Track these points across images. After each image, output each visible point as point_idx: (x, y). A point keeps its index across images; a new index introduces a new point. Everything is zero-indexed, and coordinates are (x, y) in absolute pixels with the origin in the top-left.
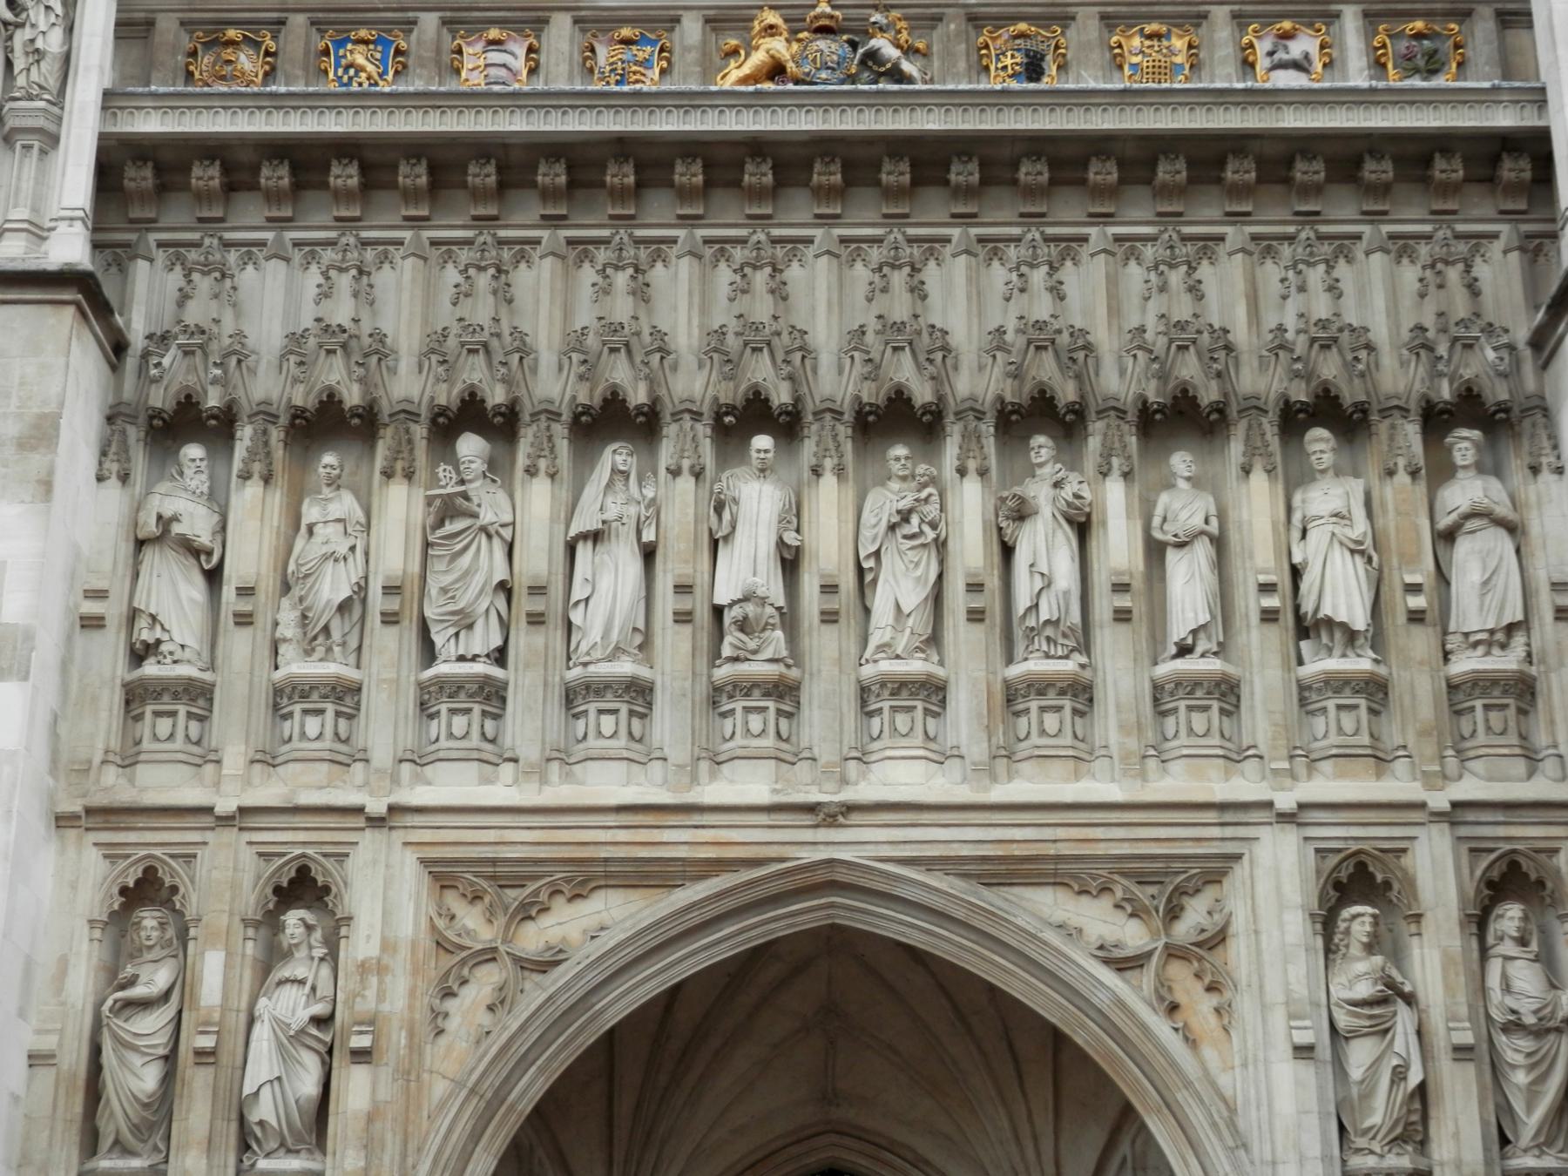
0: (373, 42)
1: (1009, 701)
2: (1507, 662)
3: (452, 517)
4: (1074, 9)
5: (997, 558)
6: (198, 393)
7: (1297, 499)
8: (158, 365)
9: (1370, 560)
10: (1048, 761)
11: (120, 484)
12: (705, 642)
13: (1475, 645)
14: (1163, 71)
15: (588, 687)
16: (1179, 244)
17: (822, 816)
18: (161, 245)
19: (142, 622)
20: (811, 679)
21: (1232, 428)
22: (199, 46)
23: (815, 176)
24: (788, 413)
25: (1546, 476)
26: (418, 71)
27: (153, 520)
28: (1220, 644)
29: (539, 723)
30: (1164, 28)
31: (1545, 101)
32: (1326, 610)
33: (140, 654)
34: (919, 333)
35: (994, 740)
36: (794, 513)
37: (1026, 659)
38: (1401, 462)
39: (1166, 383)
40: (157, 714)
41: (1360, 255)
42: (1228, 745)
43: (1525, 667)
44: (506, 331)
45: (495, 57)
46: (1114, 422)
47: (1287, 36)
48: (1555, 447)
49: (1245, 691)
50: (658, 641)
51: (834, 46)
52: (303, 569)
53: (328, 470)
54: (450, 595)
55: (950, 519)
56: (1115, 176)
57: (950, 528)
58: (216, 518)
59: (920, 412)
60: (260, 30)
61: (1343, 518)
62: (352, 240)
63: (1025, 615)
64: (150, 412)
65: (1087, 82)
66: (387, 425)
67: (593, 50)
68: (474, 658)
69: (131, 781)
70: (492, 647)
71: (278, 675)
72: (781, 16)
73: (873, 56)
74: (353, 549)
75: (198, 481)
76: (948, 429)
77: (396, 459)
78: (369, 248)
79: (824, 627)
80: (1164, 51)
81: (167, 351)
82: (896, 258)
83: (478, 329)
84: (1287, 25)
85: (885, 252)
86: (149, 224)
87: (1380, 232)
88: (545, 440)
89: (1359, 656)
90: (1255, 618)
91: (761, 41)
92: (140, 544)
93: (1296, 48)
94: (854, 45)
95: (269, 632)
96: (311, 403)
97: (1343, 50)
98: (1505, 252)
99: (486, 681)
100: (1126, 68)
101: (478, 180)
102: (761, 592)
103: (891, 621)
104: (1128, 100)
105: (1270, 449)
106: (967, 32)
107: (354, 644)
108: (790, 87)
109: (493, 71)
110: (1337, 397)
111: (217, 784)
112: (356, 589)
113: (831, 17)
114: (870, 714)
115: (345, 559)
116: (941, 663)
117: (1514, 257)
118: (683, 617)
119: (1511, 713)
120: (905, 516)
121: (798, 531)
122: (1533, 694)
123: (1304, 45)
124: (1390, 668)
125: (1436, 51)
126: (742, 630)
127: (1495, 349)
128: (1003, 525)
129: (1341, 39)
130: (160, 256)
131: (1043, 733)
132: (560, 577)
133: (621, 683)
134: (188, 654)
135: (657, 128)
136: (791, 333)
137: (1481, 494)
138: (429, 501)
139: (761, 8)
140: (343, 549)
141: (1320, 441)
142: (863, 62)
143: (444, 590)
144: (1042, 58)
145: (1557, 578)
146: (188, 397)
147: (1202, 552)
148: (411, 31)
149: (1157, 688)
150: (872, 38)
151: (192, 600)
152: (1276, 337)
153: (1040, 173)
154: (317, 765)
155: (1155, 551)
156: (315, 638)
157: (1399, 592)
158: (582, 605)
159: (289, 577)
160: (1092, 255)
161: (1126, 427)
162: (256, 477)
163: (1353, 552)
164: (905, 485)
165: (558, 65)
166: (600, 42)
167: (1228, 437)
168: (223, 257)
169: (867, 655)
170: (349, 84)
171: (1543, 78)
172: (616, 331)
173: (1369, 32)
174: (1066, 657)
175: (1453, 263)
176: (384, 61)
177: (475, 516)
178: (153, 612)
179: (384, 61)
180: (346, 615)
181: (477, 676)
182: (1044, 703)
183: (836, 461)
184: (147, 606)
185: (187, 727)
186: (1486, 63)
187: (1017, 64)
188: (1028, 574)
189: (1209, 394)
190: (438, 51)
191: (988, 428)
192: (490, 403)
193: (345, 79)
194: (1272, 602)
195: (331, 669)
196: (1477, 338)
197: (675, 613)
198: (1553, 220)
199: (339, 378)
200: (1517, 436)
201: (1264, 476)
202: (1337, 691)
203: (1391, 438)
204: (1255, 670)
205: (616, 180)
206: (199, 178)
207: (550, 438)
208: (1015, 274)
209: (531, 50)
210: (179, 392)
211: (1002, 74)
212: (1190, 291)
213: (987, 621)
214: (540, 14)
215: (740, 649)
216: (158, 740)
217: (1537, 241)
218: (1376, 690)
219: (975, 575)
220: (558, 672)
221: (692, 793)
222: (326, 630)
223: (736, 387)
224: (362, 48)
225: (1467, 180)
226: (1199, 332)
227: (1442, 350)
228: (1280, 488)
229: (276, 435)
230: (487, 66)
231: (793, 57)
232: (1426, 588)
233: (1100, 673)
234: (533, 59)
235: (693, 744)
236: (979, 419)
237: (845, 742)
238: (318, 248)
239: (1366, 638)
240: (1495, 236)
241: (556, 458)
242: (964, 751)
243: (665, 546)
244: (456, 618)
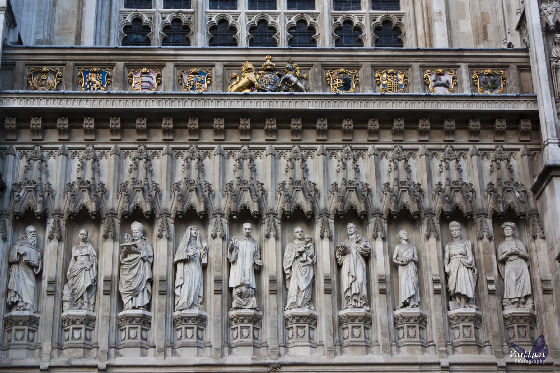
0: (99, 73)
1: (340, 324)
2: (526, 309)
3: (130, 254)
4: (362, 63)
5: (335, 270)
6: (33, 206)
7: (447, 248)
8: (18, 196)
9: (474, 271)
10: (355, 347)
11: (3, 241)
12: (226, 301)
13: (514, 303)
14: (395, 87)
15: (182, 319)
16: (401, 152)
17: (271, 368)
18: (18, 149)
19: (11, 294)
20: (266, 316)
21: (422, 221)
22: (32, 73)
23: (266, 125)
24: (257, 215)
25: (539, 240)
26: (116, 84)
27: (16, 255)
28: (419, 302)
29: (164, 333)
30: (395, 71)
31: (537, 101)
32: (458, 290)
33: (10, 306)
34: (306, 185)
35: (335, 339)
36: (259, 252)
37: (347, 308)
38: (485, 234)
39: (397, 205)
40: (17, 330)
41: (469, 157)
42: (423, 341)
43: (532, 312)
44: (150, 183)
45: (145, 79)
46: (379, 218)
47: (441, 74)
48: (542, 229)
49: (428, 320)
50: (208, 301)
51: (273, 76)
52: (73, 274)
53: (83, 236)
54: (129, 283)
55: (317, 255)
56: (378, 126)
57: (318, 258)
58: (39, 254)
59: (306, 214)
60: (56, 68)
61: (464, 255)
62: (91, 148)
63: (346, 291)
64: (15, 214)
65: (367, 91)
66: (105, 218)
67: (182, 76)
68: (139, 308)
69: (7, 356)
70: (145, 304)
71: (63, 315)
72: (252, 64)
73: (287, 80)
74: (92, 266)
75: (31, 240)
76: (316, 221)
77: (109, 231)
78: (97, 151)
79: (271, 296)
80: (395, 79)
81: (21, 190)
82: (296, 156)
83: (140, 182)
84: (440, 70)
85: (292, 154)
86: (15, 141)
87: (476, 148)
88: (165, 225)
89: (471, 307)
90: (432, 293)
91: (245, 74)
92: (10, 264)
93: (444, 79)
94: (280, 76)
95: (60, 298)
96: (77, 210)
97: (461, 79)
98: (522, 156)
99: (144, 316)
100: (381, 85)
101: (139, 126)
102: (247, 283)
103: (296, 294)
104: (383, 99)
105: (436, 229)
106: (322, 72)
107: (92, 302)
108: (256, 92)
109: (144, 84)
110: (461, 210)
111: (40, 357)
112: (93, 281)
113: (271, 65)
114: (289, 329)
115: (89, 270)
116: (315, 309)
117: (525, 158)
118: (217, 292)
119: (527, 329)
120: (301, 254)
121: (260, 259)
122: (536, 322)
123: (447, 77)
124: (482, 312)
125: (495, 81)
126: (240, 297)
127: (519, 192)
128: (338, 257)
129: (460, 76)
130: (18, 153)
131: (353, 336)
132: (171, 277)
133: (195, 317)
134: (28, 307)
135: (207, 107)
136: (257, 184)
137: (515, 247)
138: (122, 247)
139: (245, 61)
140: (88, 266)
141: (455, 226)
142: (283, 82)
143: (127, 282)
144: (350, 81)
145: (543, 278)
146: (29, 208)
147: (412, 267)
148: (113, 68)
149: (396, 319)
150: (286, 73)
151: (30, 286)
152: (438, 187)
153: (350, 125)
154: (79, 349)
155: (394, 267)
156: (77, 300)
157: (485, 284)
158: (179, 287)
159: (68, 277)
160: (369, 156)
161: (383, 220)
162: (55, 238)
163: (468, 268)
164: (300, 242)
165: (169, 82)
166: (185, 73)
167: (421, 224)
168: (42, 154)
169: (287, 306)
170: (90, 88)
171: (535, 93)
172: (192, 183)
173: (470, 74)
174: (362, 307)
175: (503, 160)
176: (103, 80)
177: (140, 253)
178: (16, 290)
179: (103, 80)
180: (90, 292)
181: (140, 314)
182: (354, 325)
183: (275, 233)
184: (13, 288)
185: (28, 335)
186: (514, 85)
187: (340, 84)
188: (347, 276)
189: (413, 208)
190: (124, 76)
191: (331, 220)
192: (144, 211)
193: (88, 86)
194: (438, 287)
195: (83, 312)
196: (513, 189)
197: (215, 291)
198: (540, 144)
199: (87, 201)
200: (527, 225)
201: (435, 239)
202: (463, 321)
203: (481, 225)
204: (432, 312)
205: (192, 126)
206: (33, 125)
207: (167, 224)
208: (341, 162)
209: (158, 76)
210: (25, 206)
211: (335, 87)
212: (406, 169)
213: (332, 294)
214: (162, 63)
215: (239, 304)
216: (18, 340)
217: (534, 152)
218: (477, 319)
219: (328, 276)
220: (170, 313)
221: (222, 360)
222: (82, 297)
223: (237, 205)
224: (94, 75)
225: (507, 129)
226: (410, 185)
227: (500, 193)
228: (440, 243)
229: (63, 222)
230: (142, 82)
231: (257, 80)
232: (495, 282)
233: (375, 314)
234: (159, 80)
235: (222, 341)
236: (328, 217)
237: (280, 340)
238: (78, 151)
239: (473, 300)
240: (518, 150)
241: (169, 231)
242: (324, 343)
243: (210, 265)
244: (132, 292)
